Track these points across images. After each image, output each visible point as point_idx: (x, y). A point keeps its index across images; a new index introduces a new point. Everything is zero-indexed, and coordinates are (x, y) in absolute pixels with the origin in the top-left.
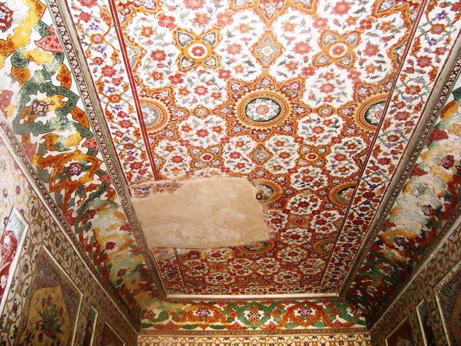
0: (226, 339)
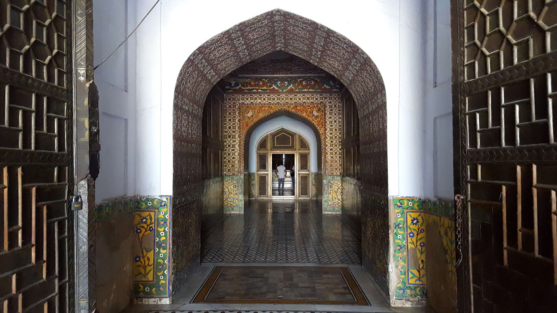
0: (269, 96)
